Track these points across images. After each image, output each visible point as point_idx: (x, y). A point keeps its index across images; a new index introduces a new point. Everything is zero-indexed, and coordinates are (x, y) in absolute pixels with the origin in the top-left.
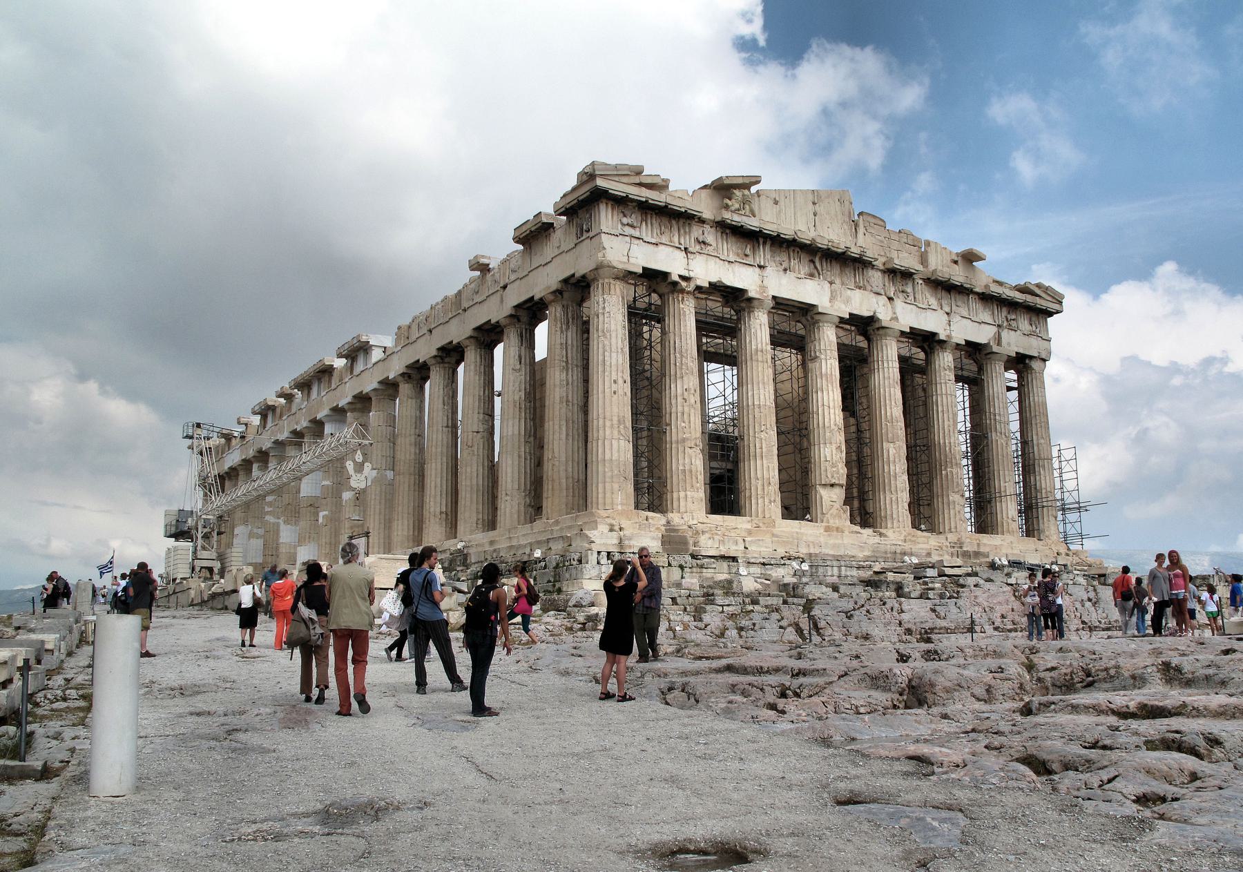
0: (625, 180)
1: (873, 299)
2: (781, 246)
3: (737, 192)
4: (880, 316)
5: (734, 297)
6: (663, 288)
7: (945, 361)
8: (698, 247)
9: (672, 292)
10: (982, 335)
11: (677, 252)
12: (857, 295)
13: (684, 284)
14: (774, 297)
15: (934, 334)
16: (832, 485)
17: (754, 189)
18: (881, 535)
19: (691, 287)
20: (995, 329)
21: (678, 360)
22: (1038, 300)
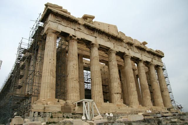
0: (56, 8)
1: (124, 49)
2: (101, 33)
3: (88, 19)
4: (125, 52)
5: (89, 44)
6: (68, 39)
7: (142, 65)
8: (78, 30)
9: (71, 39)
10: (149, 60)
11: (72, 29)
12: (120, 47)
13: (74, 37)
14: (99, 45)
15: (138, 58)
16: (118, 93)
17: (94, 20)
18: (132, 107)
19: (76, 38)
20: (151, 59)
21: (72, 56)
22: (159, 53)
